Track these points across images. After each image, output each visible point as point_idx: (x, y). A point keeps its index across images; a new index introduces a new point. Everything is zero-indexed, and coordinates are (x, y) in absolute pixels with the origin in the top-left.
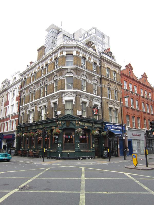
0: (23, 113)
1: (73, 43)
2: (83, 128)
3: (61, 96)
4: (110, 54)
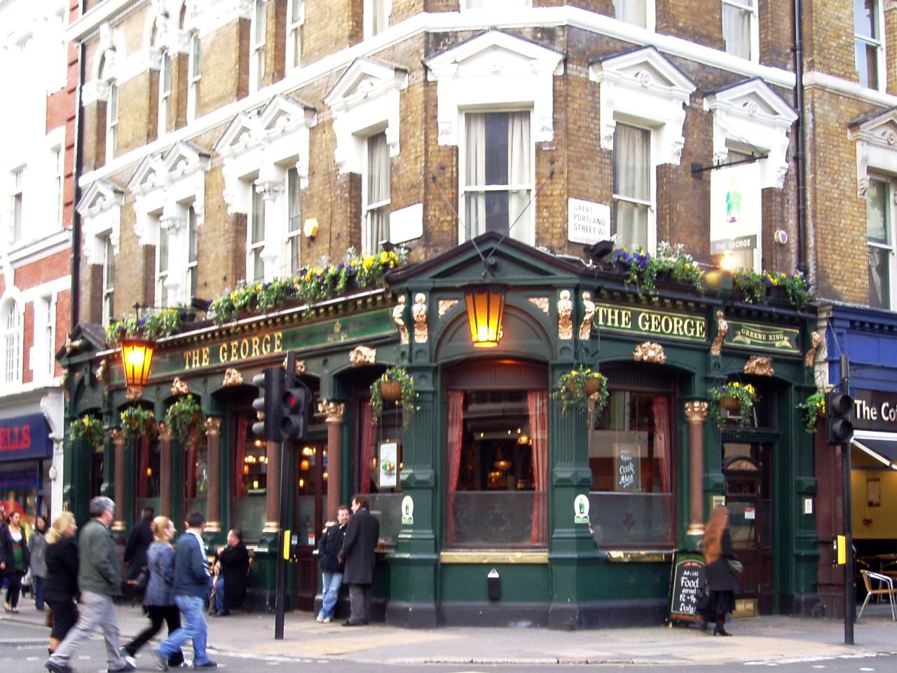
2: (614, 353)
3: (426, 68)
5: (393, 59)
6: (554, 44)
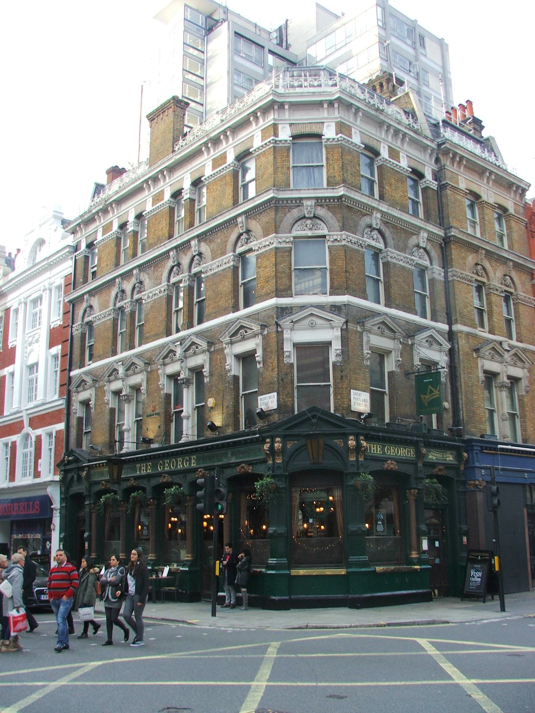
1: (320, 86)
3: (277, 325)
4: (476, 127)
5: (258, 320)
6: (340, 313)
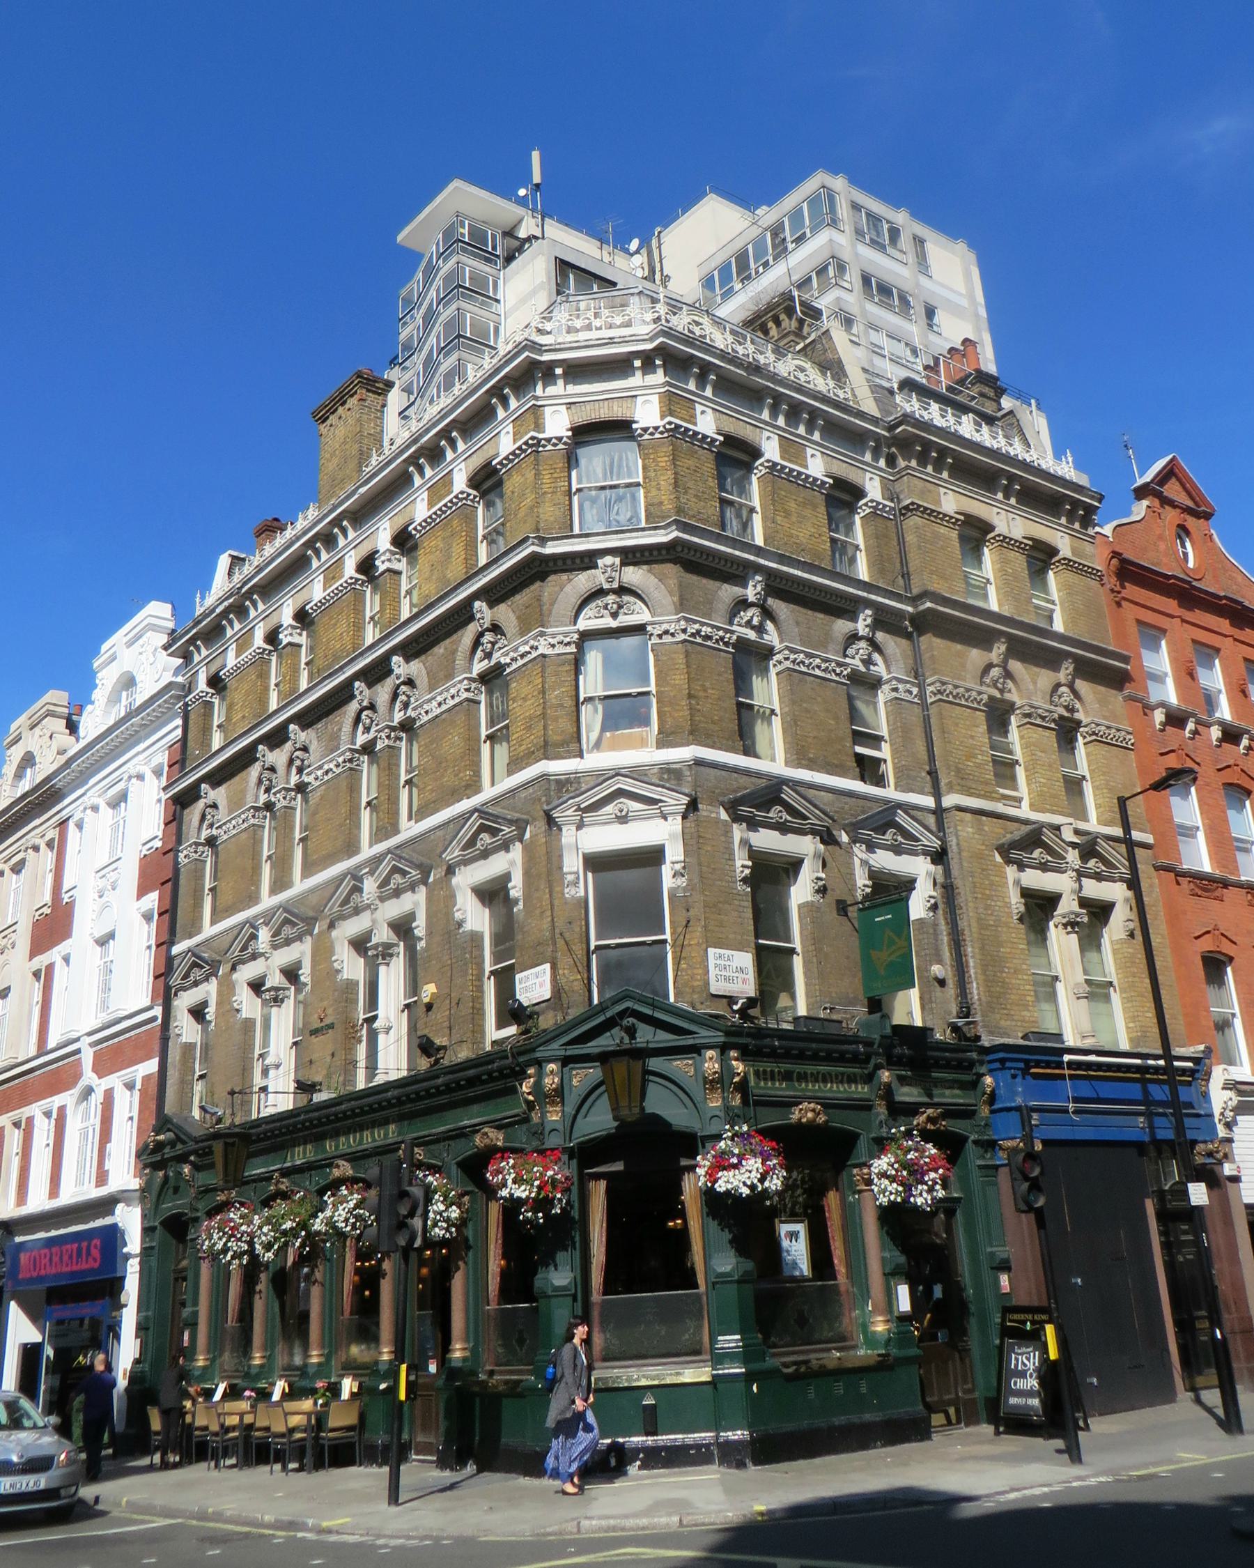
0: (198, 1013)
1: (628, 325)
2: (772, 1119)
4: (987, 390)
